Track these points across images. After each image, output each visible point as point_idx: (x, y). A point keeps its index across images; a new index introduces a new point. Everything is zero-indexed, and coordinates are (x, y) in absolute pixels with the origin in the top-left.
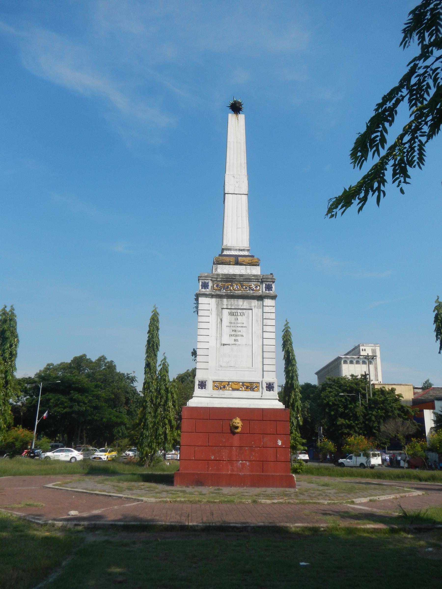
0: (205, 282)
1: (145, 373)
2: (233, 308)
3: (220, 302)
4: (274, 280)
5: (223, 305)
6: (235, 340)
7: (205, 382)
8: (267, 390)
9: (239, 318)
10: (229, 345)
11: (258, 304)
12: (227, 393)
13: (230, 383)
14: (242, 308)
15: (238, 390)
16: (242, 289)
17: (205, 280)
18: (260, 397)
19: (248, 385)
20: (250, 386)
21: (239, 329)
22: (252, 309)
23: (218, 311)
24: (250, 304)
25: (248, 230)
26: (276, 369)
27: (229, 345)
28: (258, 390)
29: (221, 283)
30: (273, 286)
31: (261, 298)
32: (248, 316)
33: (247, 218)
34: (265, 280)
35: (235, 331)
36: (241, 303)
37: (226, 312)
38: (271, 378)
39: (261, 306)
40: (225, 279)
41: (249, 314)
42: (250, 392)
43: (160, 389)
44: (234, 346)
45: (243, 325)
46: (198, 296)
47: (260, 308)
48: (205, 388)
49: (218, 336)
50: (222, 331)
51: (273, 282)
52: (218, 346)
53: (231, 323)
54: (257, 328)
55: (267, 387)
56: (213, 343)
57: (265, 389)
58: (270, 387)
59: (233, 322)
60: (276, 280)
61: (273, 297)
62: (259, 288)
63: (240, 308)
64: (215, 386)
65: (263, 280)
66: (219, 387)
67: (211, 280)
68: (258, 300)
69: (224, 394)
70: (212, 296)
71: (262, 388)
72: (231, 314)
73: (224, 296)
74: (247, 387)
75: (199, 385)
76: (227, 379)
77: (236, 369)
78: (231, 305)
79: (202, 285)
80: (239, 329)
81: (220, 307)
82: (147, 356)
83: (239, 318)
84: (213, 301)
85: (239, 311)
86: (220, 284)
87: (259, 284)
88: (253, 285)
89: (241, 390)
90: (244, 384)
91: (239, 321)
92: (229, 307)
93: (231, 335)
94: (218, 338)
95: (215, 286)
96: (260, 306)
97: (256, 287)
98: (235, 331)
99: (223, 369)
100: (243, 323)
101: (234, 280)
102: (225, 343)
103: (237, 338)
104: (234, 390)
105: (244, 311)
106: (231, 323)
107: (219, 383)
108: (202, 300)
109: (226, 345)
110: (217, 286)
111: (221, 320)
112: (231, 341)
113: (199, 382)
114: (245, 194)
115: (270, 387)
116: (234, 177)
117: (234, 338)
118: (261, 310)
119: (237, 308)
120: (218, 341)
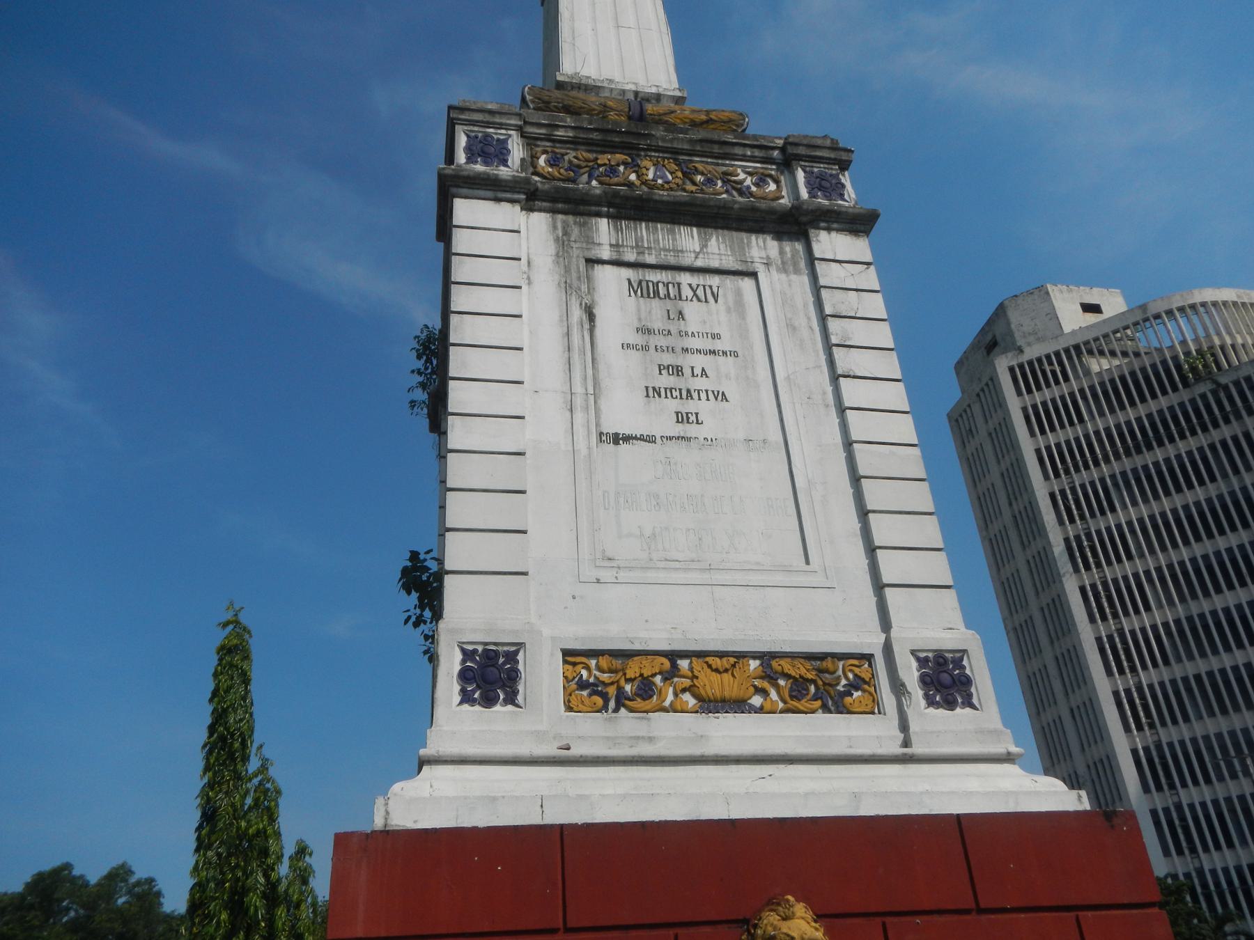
0: (487, 135)
1: (197, 850)
2: (650, 259)
3: (575, 232)
4: (844, 156)
5: (590, 242)
6: (682, 418)
7: (512, 657)
8: (931, 703)
9: (692, 310)
10: (650, 439)
11: (782, 252)
12: (672, 729)
13: (684, 664)
14: (699, 263)
15: (738, 705)
16: (690, 187)
17: (488, 124)
18: (895, 749)
19: (802, 669)
20: (819, 682)
21: (699, 361)
22: (754, 275)
23: (567, 270)
24: (742, 248)
25: (667, 40)
26: (953, 577)
27: (650, 439)
28: (874, 708)
29: (573, 154)
30: (846, 179)
31: (794, 225)
32: (739, 306)
34: (802, 151)
35: (678, 371)
36: (688, 241)
37: (610, 281)
38: (935, 620)
39: (802, 264)
40: (595, 136)
42: (820, 716)
43: (245, 891)
45: (718, 345)
46: (451, 186)
47: (797, 271)
48: (511, 699)
49: (578, 389)
51: (844, 166)
52: (581, 445)
53: (646, 331)
54: (801, 362)
55: (925, 681)
56: (546, 425)
57: (917, 693)
58: (946, 680)
59: (658, 323)
60: (854, 157)
61: (859, 223)
62: (772, 187)
63: (687, 260)
64: (582, 685)
65: (790, 150)
66: (612, 691)
67: (519, 128)
68: (779, 236)
69: (651, 739)
70: (530, 196)
71: (899, 688)
72: (643, 290)
73: (598, 201)
74: (798, 688)
75: (464, 676)
76: (657, 636)
77: (705, 578)
79: (469, 149)
80: (699, 361)
81: (576, 252)
82: (211, 785)
83: (692, 310)
85: (685, 279)
86: (571, 156)
87: (772, 169)
88: (742, 176)
89: (761, 710)
90: (774, 663)
92: (631, 256)
93: (654, 392)
94: (578, 401)
95: (542, 161)
96: (795, 264)
98: (678, 371)
99: (624, 575)
100: (716, 336)
102: (624, 430)
103: (690, 406)
104: (711, 705)
105: (715, 281)
106: (646, 331)
107: (604, 662)
108: (465, 210)
109: (628, 439)
110: (554, 161)
111: (591, 317)
112: (659, 419)
113: (467, 655)
115: (946, 680)
117: (673, 405)
118: (805, 279)
119: (672, 260)
120: (579, 417)
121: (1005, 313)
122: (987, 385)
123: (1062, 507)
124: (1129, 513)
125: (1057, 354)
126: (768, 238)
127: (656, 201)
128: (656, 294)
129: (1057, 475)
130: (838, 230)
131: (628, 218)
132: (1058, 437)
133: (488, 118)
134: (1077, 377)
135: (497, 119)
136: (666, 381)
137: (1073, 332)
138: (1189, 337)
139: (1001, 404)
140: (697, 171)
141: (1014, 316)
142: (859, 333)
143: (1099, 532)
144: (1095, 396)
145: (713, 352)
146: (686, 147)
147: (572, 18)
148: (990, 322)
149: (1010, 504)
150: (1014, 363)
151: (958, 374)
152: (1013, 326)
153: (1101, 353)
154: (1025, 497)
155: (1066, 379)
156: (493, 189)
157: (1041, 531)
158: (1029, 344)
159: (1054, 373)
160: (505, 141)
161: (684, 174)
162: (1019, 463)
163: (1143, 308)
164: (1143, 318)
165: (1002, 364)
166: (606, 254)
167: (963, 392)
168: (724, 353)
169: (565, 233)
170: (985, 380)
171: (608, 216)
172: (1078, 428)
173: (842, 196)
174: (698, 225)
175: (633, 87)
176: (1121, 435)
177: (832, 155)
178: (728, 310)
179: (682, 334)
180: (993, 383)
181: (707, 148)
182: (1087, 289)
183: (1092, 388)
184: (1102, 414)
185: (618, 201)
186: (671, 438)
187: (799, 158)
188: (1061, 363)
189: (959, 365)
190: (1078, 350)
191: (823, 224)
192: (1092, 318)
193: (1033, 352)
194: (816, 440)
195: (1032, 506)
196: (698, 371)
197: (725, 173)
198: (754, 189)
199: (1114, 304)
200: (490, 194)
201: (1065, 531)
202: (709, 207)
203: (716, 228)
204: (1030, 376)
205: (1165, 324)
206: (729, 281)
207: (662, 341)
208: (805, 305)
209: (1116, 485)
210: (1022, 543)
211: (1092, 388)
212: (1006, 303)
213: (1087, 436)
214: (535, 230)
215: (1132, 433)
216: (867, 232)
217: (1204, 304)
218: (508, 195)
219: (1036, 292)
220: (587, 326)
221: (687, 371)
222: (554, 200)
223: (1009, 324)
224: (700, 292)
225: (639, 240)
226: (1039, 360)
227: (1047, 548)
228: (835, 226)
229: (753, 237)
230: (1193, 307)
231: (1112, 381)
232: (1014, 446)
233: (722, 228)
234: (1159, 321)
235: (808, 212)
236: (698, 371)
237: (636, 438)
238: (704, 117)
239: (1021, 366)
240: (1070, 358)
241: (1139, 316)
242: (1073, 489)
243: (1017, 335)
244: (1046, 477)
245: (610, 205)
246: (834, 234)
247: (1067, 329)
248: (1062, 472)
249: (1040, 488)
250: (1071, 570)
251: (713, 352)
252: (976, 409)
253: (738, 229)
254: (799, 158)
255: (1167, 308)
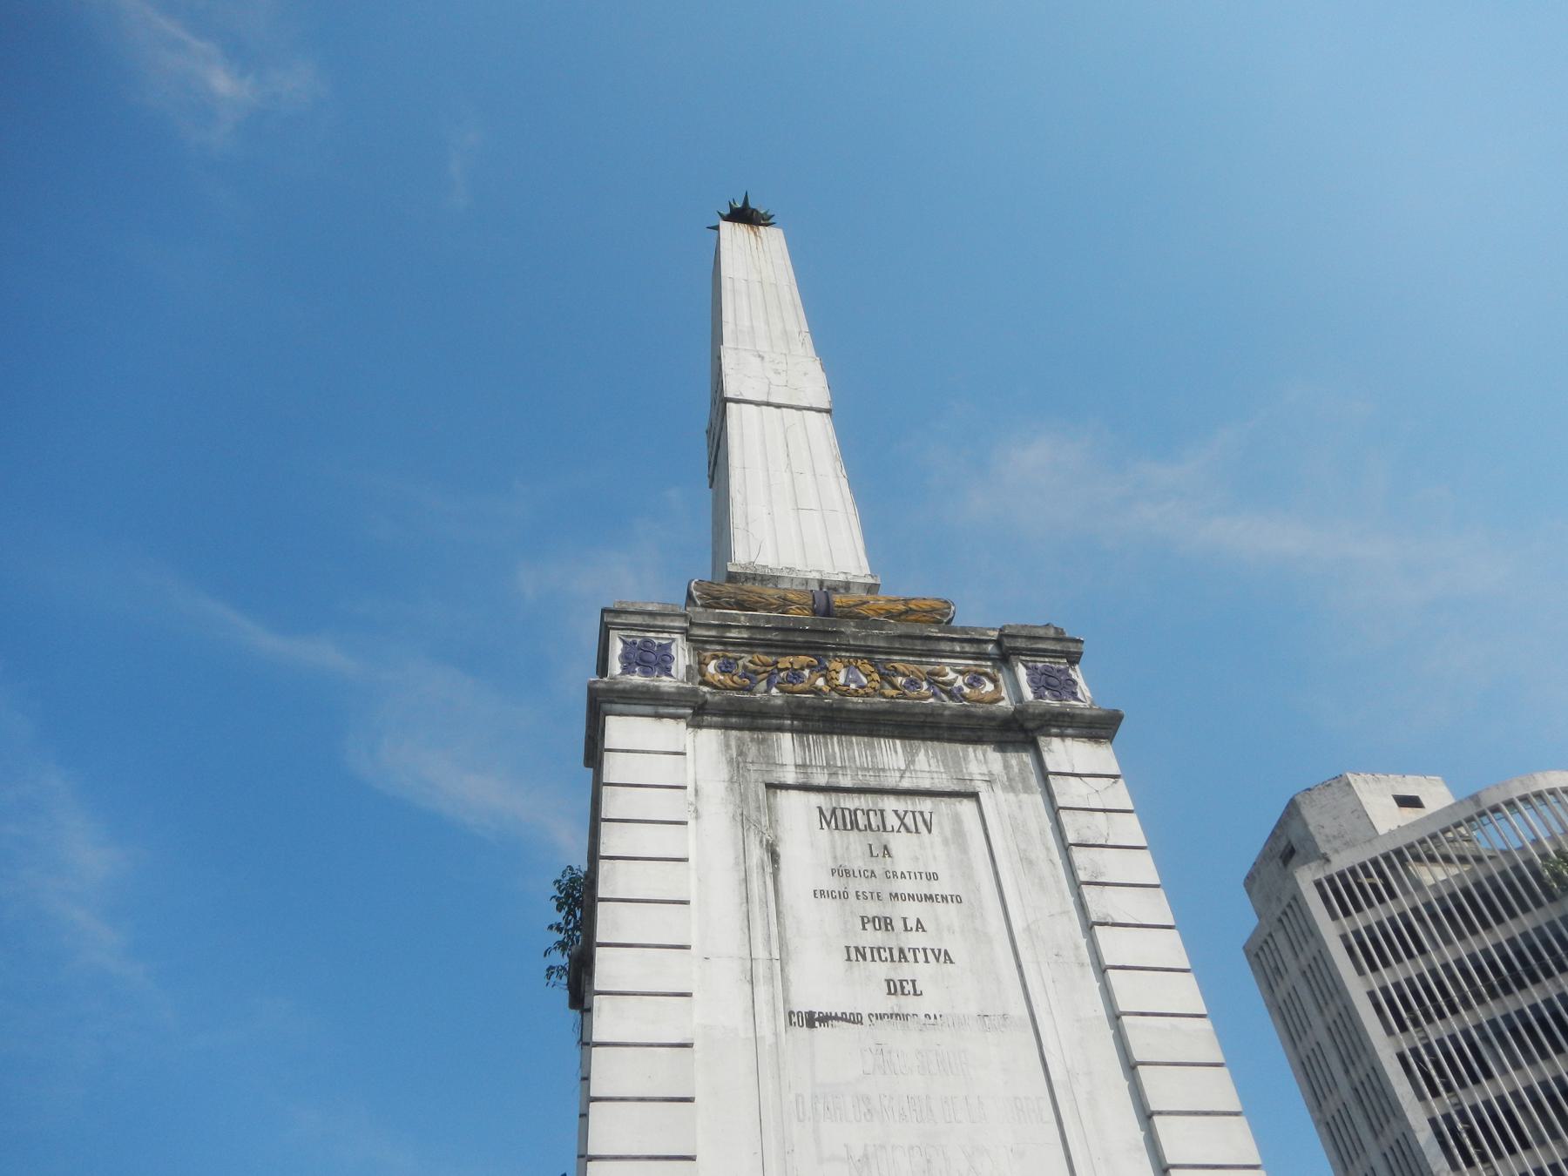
0: (647, 641)
2: (845, 781)
3: (752, 751)
4: (1072, 648)
5: (771, 762)
6: (894, 988)
9: (900, 844)
10: (854, 1019)
11: (1007, 766)
14: (906, 784)
16: (889, 691)
17: (648, 628)
22: (974, 796)
23: (744, 798)
25: (855, 521)
27: (854, 1019)
29: (748, 657)
30: (1077, 674)
31: (1018, 732)
32: (959, 833)
33: (844, 482)
34: (1021, 643)
35: (886, 924)
36: (891, 758)
37: (797, 810)
39: (1034, 780)
40: (774, 636)
41: (957, 819)
44: (889, 1033)
45: (936, 888)
46: (601, 703)
49: (760, 952)
50: (789, 921)
51: (1074, 659)
52: (765, 1029)
53: (843, 873)
56: (719, 1005)
59: (858, 863)
60: (1084, 648)
61: (1100, 727)
62: (989, 687)
63: (891, 781)
65: (1007, 643)
68: (1002, 746)
70: (698, 712)
72: (836, 820)
73: (778, 713)
78: (830, 767)
79: (625, 657)
80: (912, 910)
81: (756, 779)
83: (900, 844)
84: (707, 746)
85: (890, 804)
86: (746, 660)
88: (951, 676)
91: (902, 862)
92: (821, 779)
93: (858, 954)
94: (761, 970)
95: (711, 667)
96: (1024, 780)
97: (975, 681)
98: (886, 924)
100: (933, 877)
101: (831, 642)
102: (820, 1008)
103: (905, 971)
105: (926, 805)
106: (843, 873)
108: (619, 730)
109: (825, 1019)
110: (725, 669)
111: (774, 857)
112: (863, 990)
114: (819, 411)
116: (762, 358)
118: (1038, 799)
119: (873, 782)
120: (762, 992)
121: (1299, 813)
122: (1290, 906)
123: (1418, 1074)
124: (1511, 1080)
125: (1375, 862)
126: (989, 749)
127: (849, 711)
128: (855, 824)
129: (1403, 1028)
130: (1073, 737)
131: (817, 732)
132: (1395, 974)
133: (648, 621)
134: (1406, 892)
135: (659, 622)
136: (872, 938)
137: (1391, 832)
138: (1543, 835)
139: (1312, 932)
140: (897, 672)
141: (1311, 815)
142: (1113, 865)
143: (1475, 1109)
144: (1434, 916)
145: (929, 898)
146: (882, 644)
147: (745, 502)
148: (1282, 824)
149: (1347, 1071)
150: (1321, 876)
151: (1249, 892)
152: (1311, 828)
153: (1432, 859)
154: (1365, 1061)
155: (1393, 895)
156: (654, 703)
157: (1394, 1110)
158: (1336, 851)
159: (1374, 887)
160: (668, 647)
161: (882, 675)
162: (1349, 1011)
163: (1475, 799)
164: (1479, 812)
165: (1306, 878)
166: (790, 777)
167: (1260, 917)
168: (944, 898)
169: (741, 753)
170: (1286, 900)
171: (792, 730)
172: (1420, 960)
173: (1074, 695)
174: (901, 737)
175: (818, 576)
176: (1480, 969)
177: (1058, 647)
178: (946, 842)
179: (890, 875)
180: (1297, 899)
181: (908, 644)
182: (1399, 778)
183: (1428, 906)
184: (1448, 941)
185: (803, 712)
186: (881, 1017)
187: (1018, 652)
188: (1381, 874)
189: (1250, 881)
190: (1399, 856)
191: (1054, 730)
192: (1410, 815)
193: (1342, 861)
194: (1071, 1013)
195: (1376, 1071)
196: (912, 924)
197: (930, 673)
198: (967, 690)
199: (1437, 797)
200: (649, 709)
201: (1429, 1108)
202: (914, 715)
203: (924, 739)
204: (1345, 893)
205: (1507, 819)
206: (944, 805)
207: (864, 885)
208: (1042, 832)
209: (1486, 1039)
210: (1372, 1126)
211: (1428, 906)
212: (1299, 798)
213: (1433, 972)
214: (705, 749)
215: (1493, 965)
216: (1110, 738)
217: (1552, 792)
218: (672, 710)
219: (1334, 783)
220: (769, 870)
221: (898, 924)
222: (727, 714)
223: (1305, 825)
224: (909, 820)
225: (830, 759)
226: (1353, 871)
227: (1407, 1135)
228: (1070, 731)
229: (970, 749)
230: (1539, 795)
231: (1453, 896)
232: (1337, 989)
233: (932, 739)
234: (1498, 815)
235: (1034, 717)
236: (912, 924)
237: (836, 1018)
238: (901, 607)
239: (1330, 880)
240: (1392, 867)
241: (1472, 810)
242: (1428, 1047)
243: (1319, 840)
244: (1389, 1032)
245: (794, 717)
246: (1069, 741)
247: (1382, 829)
248: (1409, 1023)
249: (1385, 1048)
250: (1447, 1166)
251: (929, 898)
252: (1280, 938)
253: (950, 740)
254: (1018, 652)
255: (1506, 798)
